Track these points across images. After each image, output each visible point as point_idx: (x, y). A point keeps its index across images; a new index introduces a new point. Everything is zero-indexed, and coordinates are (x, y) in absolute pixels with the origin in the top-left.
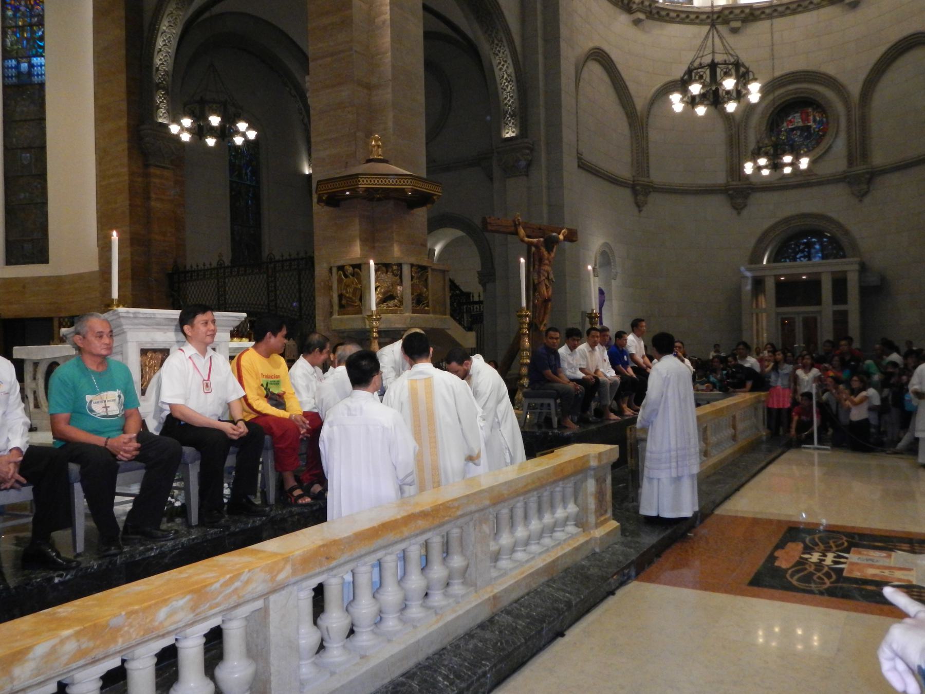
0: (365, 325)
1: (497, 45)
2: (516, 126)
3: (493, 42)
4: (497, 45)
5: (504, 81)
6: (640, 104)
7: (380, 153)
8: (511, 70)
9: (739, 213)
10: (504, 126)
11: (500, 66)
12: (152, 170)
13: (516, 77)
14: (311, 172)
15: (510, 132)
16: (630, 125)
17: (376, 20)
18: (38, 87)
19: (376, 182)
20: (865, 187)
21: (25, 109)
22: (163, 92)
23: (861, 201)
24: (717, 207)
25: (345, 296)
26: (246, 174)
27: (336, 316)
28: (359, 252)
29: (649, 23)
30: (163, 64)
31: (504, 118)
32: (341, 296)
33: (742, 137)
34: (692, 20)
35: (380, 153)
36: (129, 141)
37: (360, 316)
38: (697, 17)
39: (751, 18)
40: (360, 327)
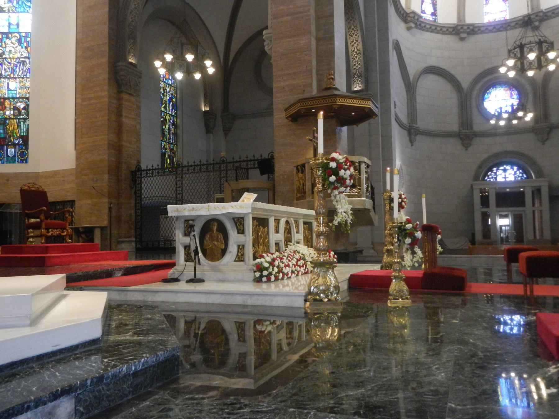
1: (353, 29)
3: (350, 27)
5: (355, 53)
8: (360, 46)
9: (467, 149)
10: (353, 83)
11: (353, 44)
12: (125, 96)
13: (364, 52)
14: (208, 109)
15: (358, 87)
16: (407, 91)
18: (24, 34)
21: (13, 50)
22: (132, 41)
23: (543, 144)
24: (453, 145)
26: (169, 107)
29: (415, 31)
30: (132, 21)
33: (468, 103)
34: (438, 31)
36: (109, 73)
38: (441, 29)
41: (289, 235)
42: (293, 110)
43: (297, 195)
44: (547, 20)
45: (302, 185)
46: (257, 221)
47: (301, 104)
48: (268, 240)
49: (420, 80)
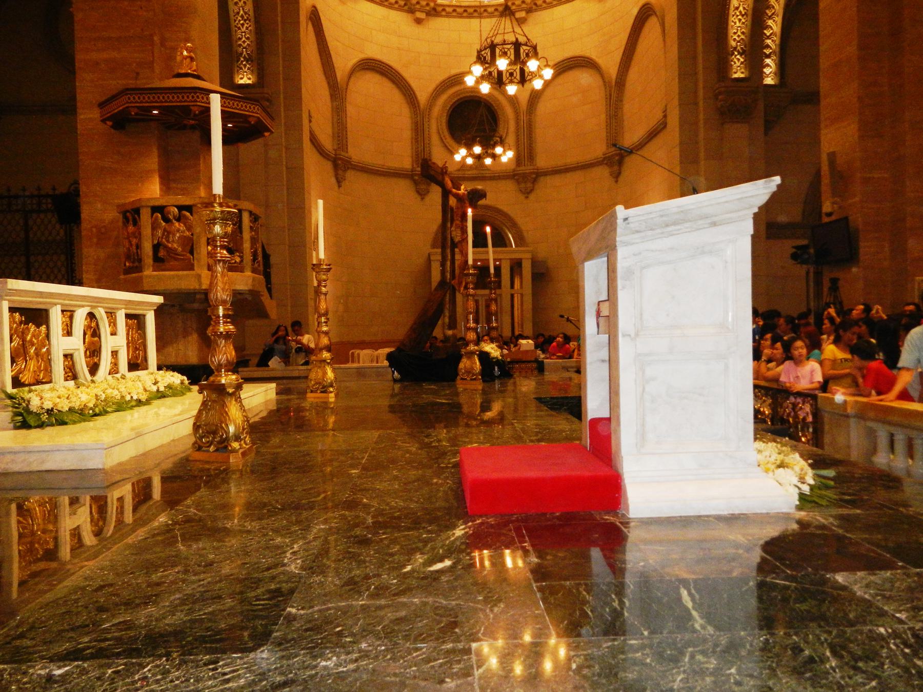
0: (200, 284)
5: (239, 18)
6: (339, 75)
8: (249, 7)
9: (422, 199)
10: (238, 71)
13: (255, 17)
16: (331, 96)
20: (529, 185)
23: (527, 197)
25: (166, 247)
28: (158, 192)
31: (238, 61)
32: (156, 248)
33: (426, 125)
35: (194, 68)
37: (191, 272)
39: (433, 12)
40: (192, 288)
41: (96, 339)
42: (116, 108)
43: (125, 265)
44: (536, 10)
45: (134, 247)
46: (21, 315)
47: (129, 98)
48: (49, 351)
49: (352, 80)
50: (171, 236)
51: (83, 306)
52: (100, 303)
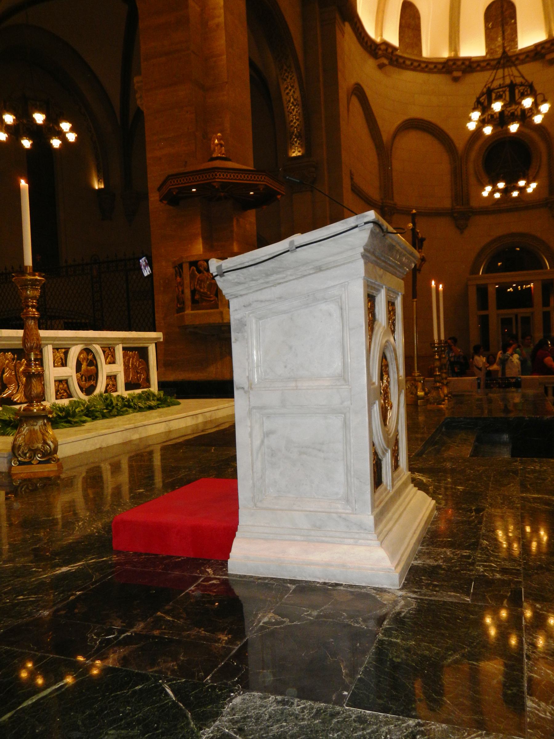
0: (223, 320)
1: (286, 70)
2: (301, 147)
4: (286, 70)
5: (291, 105)
6: (385, 137)
7: (223, 152)
8: (297, 95)
9: (462, 233)
11: (287, 91)
14: (102, 186)
16: (379, 155)
17: (209, 23)
19: (232, 176)
25: (199, 292)
27: (188, 311)
28: (202, 250)
29: (390, 69)
31: (291, 139)
32: (193, 292)
34: (423, 68)
35: (223, 152)
38: (427, 66)
40: (217, 322)
43: (177, 306)
50: (202, 284)
51: (77, 344)
52: (93, 341)
